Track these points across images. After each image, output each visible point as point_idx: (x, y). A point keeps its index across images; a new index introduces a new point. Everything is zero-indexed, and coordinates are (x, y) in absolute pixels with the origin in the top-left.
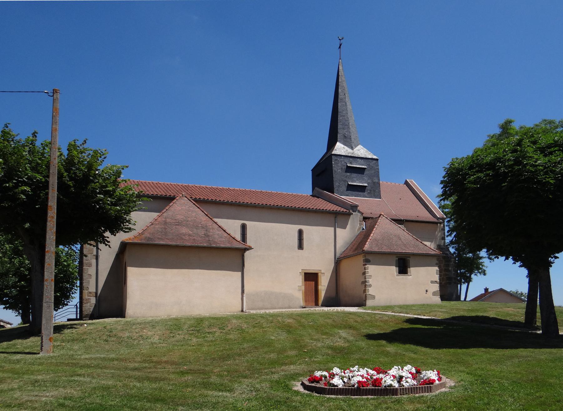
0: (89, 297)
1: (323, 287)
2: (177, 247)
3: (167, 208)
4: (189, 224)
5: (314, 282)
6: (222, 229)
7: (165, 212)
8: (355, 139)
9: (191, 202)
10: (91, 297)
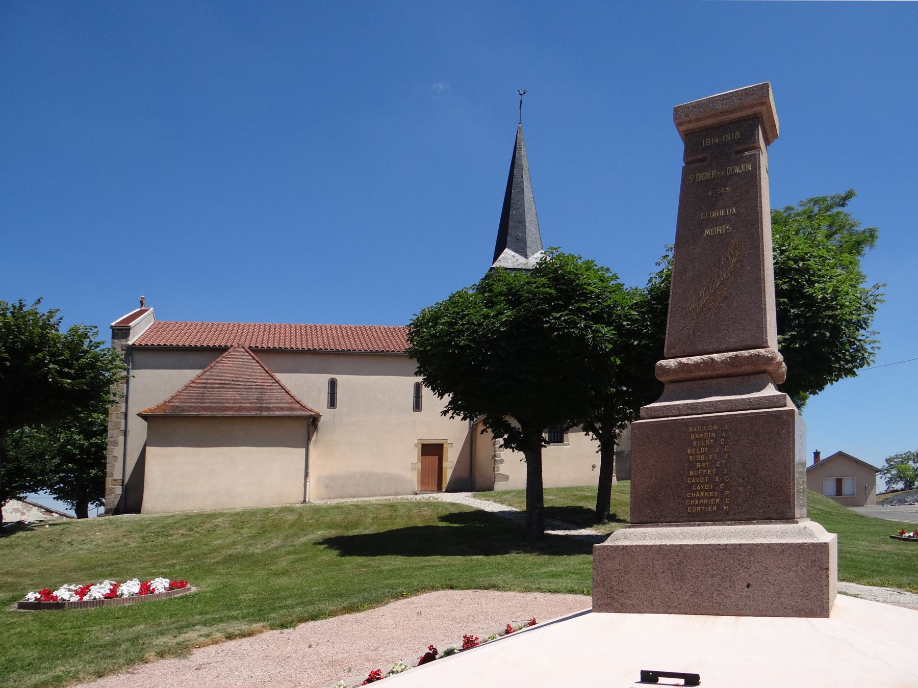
0: (114, 487)
1: (449, 464)
2: (213, 418)
3: (212, 365)
4: (239, 385)
5: (437, 457)
6: (284, 390)
7: (209, 370)
8: (533, 242)
9: (249, 354)
10: (116, 485)
